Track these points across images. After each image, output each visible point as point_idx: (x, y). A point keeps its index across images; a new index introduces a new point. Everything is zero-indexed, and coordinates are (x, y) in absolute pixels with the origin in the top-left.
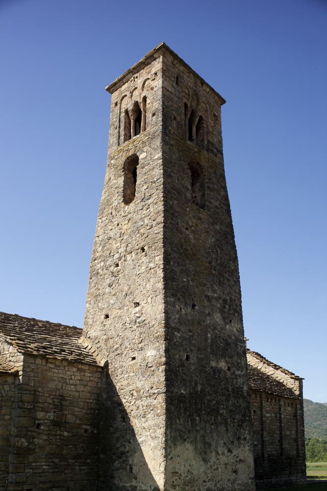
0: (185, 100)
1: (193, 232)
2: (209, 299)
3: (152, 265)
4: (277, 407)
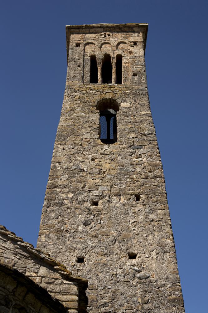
3: (152, 217)
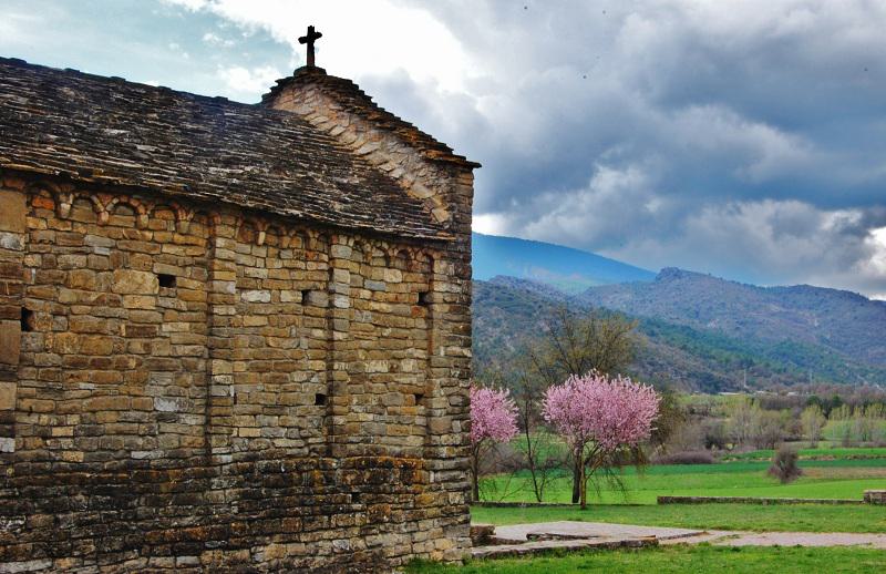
4: (312, 266)
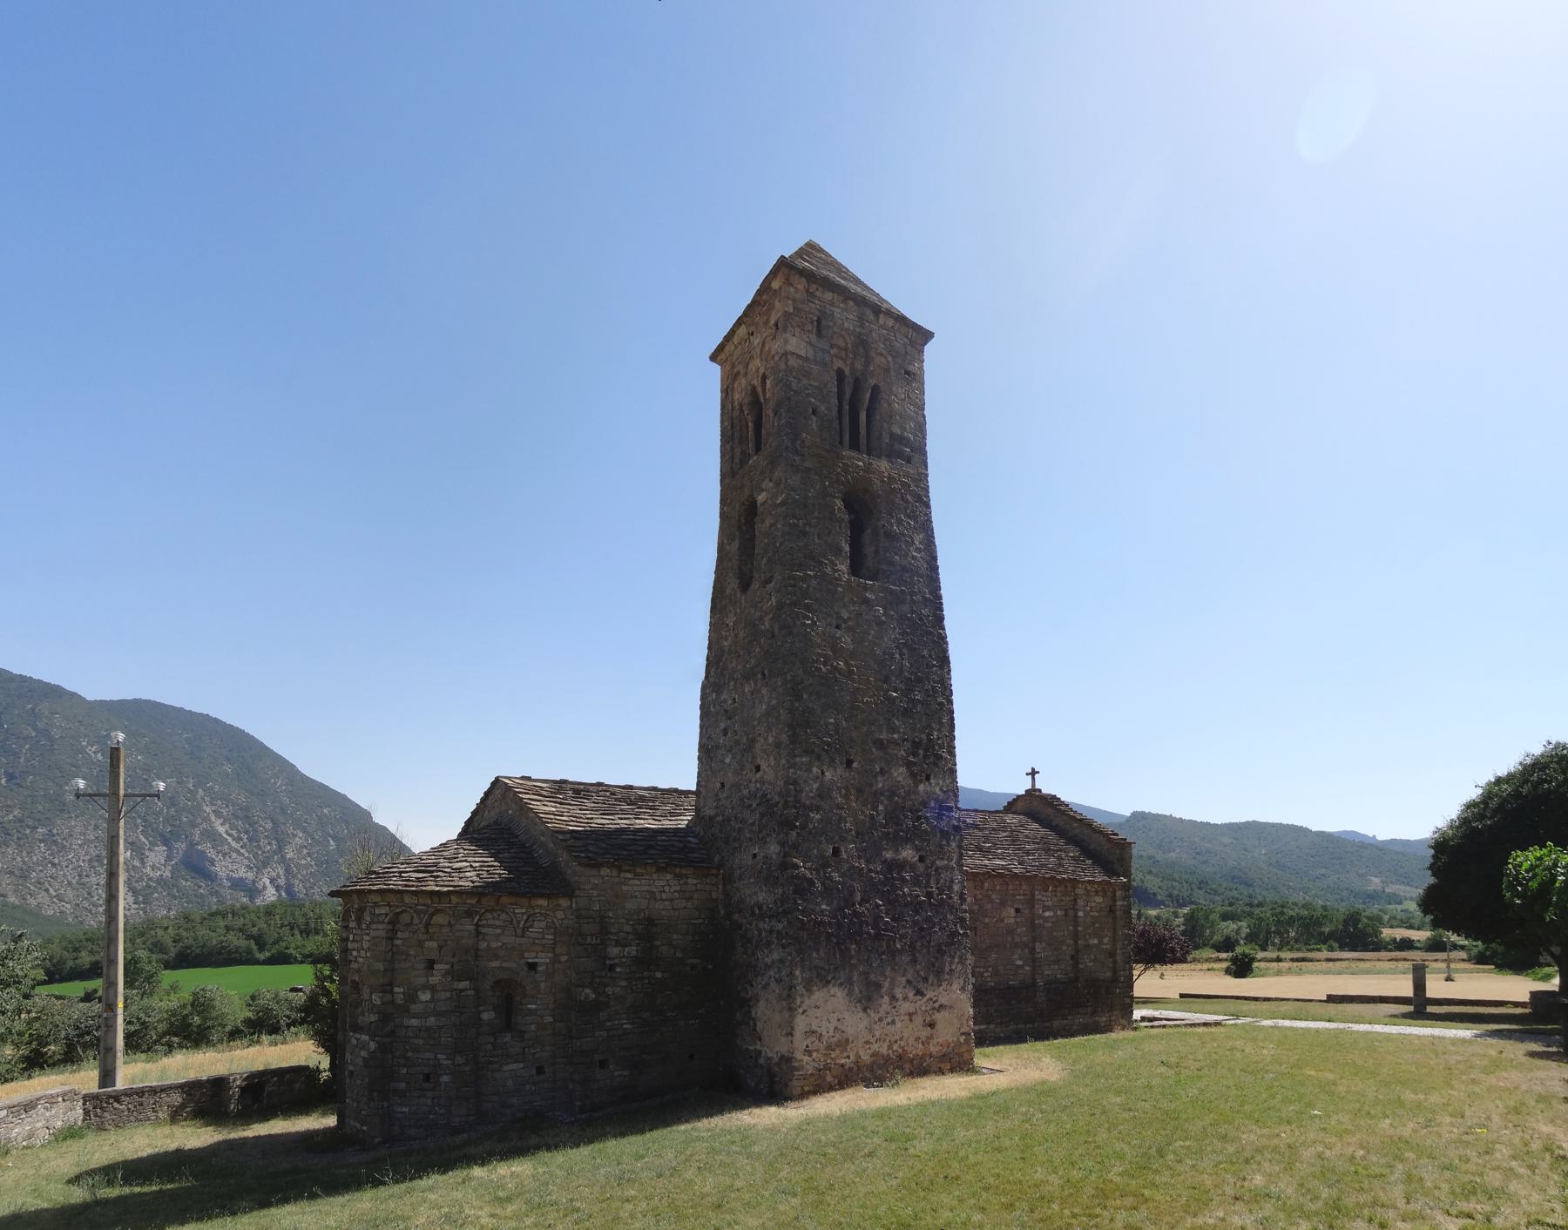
0: (839, 364)
1: (850, 629)
2: (880, 745)
